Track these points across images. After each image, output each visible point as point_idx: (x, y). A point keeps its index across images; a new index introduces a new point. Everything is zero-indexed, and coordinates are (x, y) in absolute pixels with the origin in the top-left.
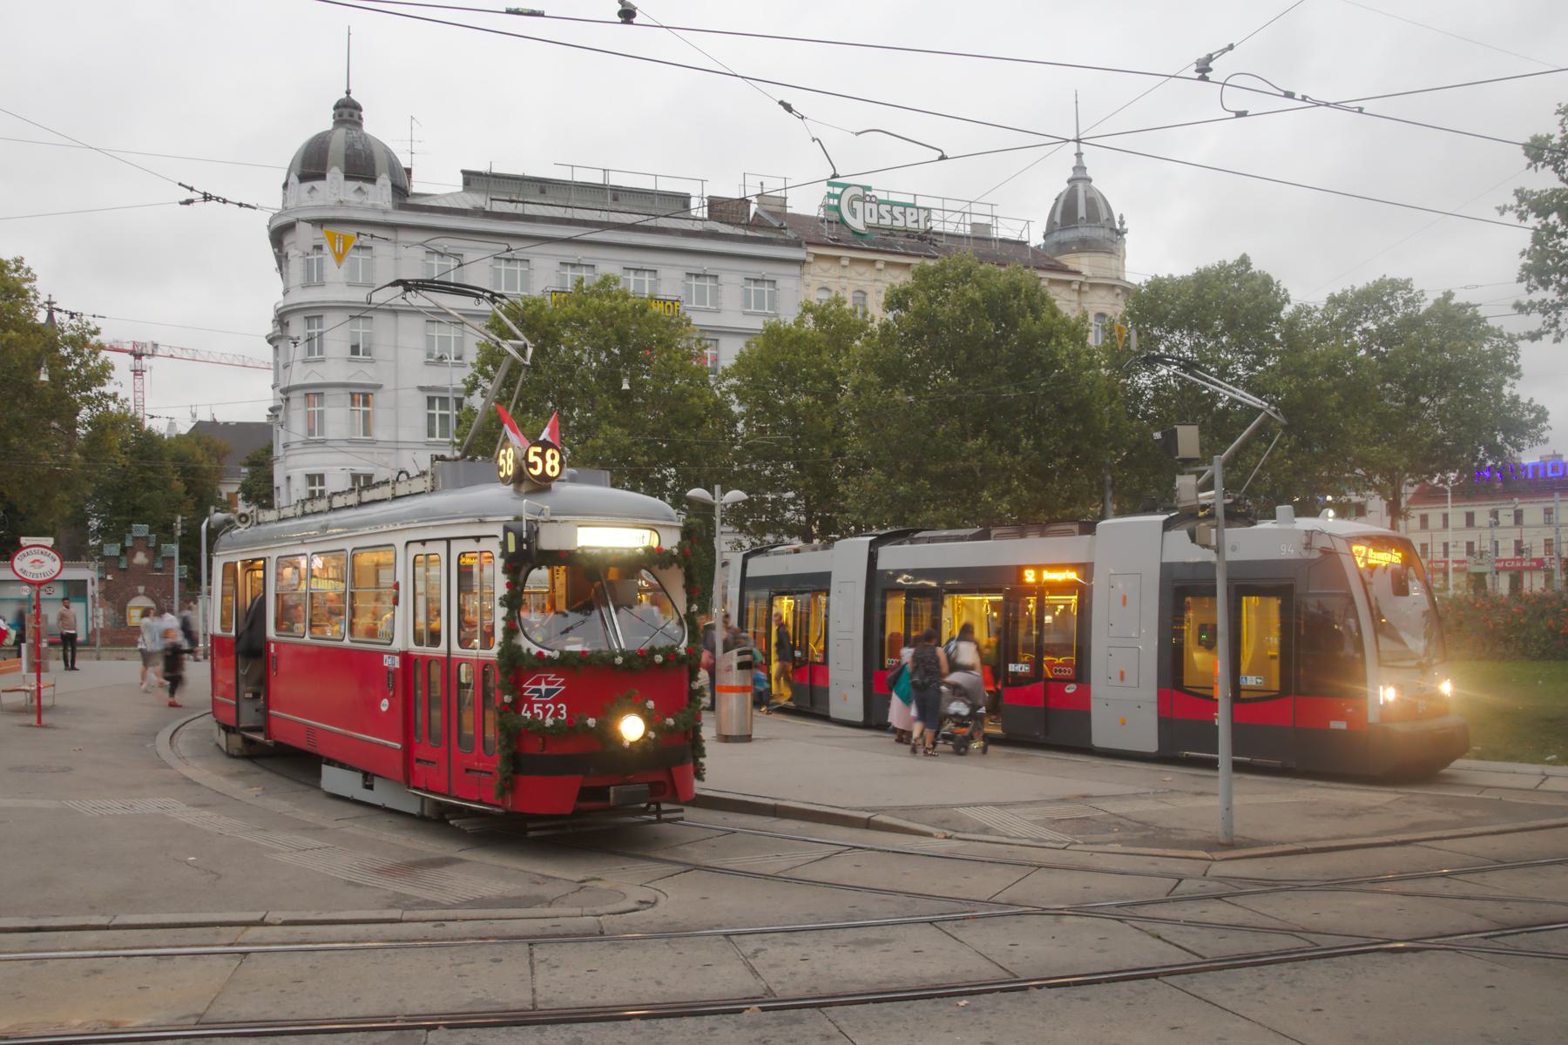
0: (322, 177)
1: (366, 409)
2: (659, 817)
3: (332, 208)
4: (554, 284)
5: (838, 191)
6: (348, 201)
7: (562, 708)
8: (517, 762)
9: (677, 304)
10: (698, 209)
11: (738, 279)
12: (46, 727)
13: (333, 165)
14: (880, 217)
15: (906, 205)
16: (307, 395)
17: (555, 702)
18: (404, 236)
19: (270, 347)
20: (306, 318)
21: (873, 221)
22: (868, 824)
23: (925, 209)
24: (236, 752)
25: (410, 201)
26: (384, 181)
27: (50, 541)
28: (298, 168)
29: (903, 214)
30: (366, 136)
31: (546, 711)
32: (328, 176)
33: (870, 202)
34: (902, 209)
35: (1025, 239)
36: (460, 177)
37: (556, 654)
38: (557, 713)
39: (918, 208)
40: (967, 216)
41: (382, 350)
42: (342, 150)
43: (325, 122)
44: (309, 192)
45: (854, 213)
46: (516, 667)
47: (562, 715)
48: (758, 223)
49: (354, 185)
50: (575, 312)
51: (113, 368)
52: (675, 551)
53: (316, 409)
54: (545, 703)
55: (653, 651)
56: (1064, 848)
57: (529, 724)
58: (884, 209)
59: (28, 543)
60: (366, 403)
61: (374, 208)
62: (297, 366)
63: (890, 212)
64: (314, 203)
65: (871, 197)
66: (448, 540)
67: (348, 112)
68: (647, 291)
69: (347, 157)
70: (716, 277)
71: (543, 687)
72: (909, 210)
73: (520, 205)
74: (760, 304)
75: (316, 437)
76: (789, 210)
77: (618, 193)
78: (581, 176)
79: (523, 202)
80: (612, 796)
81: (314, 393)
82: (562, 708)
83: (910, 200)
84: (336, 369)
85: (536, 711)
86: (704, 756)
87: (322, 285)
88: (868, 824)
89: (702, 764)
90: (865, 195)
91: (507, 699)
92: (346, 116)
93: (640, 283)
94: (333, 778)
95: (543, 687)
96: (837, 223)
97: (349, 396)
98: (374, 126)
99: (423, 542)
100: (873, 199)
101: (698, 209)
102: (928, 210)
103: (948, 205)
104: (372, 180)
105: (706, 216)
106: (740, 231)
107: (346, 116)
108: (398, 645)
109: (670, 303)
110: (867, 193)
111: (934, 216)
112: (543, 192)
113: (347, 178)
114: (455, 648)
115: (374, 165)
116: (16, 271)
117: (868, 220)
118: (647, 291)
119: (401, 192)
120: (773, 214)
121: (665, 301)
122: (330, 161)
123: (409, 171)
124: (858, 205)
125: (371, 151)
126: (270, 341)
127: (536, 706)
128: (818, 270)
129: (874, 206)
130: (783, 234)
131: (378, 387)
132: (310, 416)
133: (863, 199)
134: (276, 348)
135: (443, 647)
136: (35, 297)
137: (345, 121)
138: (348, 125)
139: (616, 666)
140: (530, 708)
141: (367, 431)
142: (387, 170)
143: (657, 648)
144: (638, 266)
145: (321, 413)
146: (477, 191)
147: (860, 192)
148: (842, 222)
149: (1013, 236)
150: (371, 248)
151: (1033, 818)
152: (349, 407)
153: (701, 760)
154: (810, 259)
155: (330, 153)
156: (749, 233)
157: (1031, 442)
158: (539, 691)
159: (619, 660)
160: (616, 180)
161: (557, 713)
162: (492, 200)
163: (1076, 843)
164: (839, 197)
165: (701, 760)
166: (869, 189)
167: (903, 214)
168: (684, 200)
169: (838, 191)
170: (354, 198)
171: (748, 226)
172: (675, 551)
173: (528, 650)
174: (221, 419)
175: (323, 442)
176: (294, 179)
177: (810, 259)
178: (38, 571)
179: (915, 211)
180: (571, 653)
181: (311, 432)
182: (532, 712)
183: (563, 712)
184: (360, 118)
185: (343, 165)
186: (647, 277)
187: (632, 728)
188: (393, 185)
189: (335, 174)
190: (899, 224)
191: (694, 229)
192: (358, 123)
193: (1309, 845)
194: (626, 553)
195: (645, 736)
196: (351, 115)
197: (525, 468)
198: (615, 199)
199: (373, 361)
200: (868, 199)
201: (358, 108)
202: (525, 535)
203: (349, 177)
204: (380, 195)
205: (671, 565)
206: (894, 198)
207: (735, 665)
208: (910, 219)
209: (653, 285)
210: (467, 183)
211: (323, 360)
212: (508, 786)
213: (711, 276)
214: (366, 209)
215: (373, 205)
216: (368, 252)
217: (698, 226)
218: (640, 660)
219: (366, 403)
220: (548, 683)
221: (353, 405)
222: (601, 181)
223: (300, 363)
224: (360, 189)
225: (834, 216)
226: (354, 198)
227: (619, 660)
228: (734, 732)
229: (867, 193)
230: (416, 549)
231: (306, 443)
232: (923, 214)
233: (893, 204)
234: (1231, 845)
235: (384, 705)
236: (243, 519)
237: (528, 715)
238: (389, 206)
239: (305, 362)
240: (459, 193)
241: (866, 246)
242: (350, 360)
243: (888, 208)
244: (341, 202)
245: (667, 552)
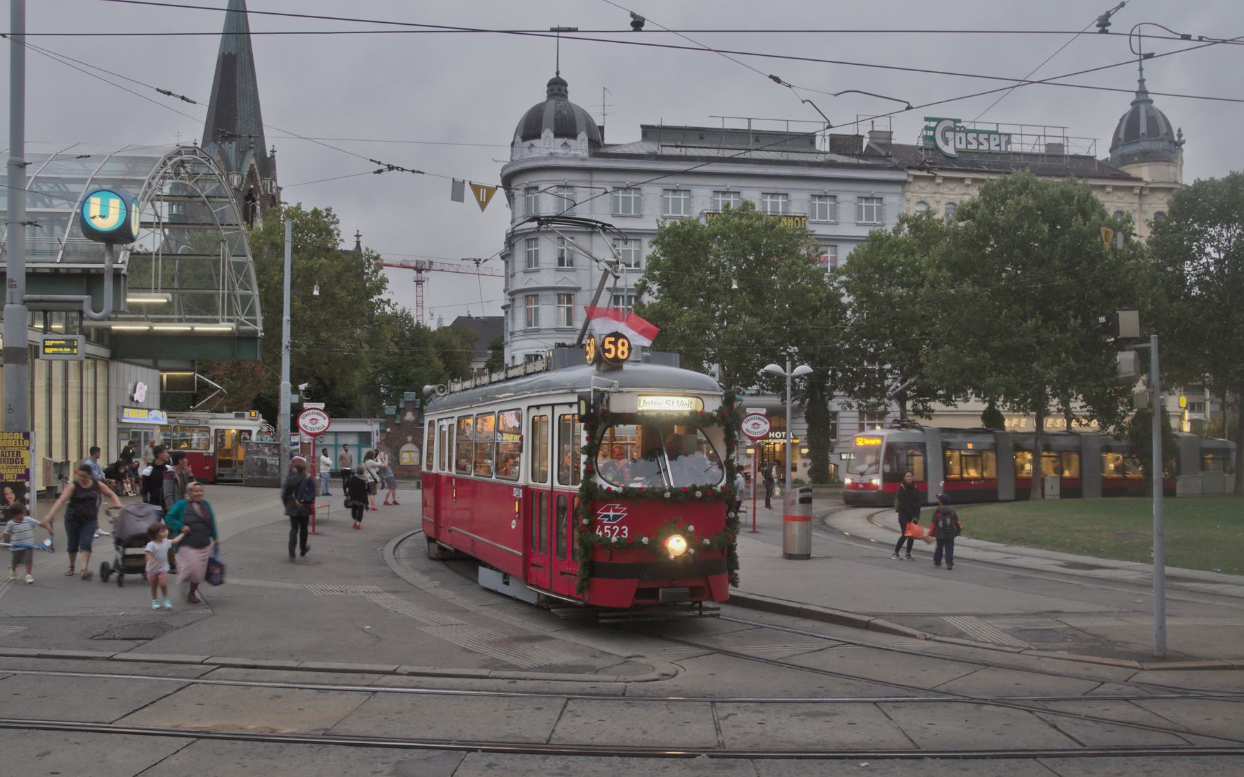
0: (538, 136)
1: (569, 305)
2: (700, 614)
3: (545, 159)
4: (709, 207)
5: (933, 124)
6: (557, 153)
7: (624, 529)
8: (592, 569)
9: (803, 219)
10: (822, 145)
11: (852, 198)
12: (317, 534)
14: (968, 143)
15: (989, 133)
16: (527, 296)
17: (620, 525)
18: (597, 177)
19: (503, 262)
21: (963, 146)
22: (868, 626)
23: (1006, 134)
24: (433, 556)
25: (602, 150)
26: (583, 136)
27: (322, 406)
28: (521, 131)
29: (988, 140)
30: (570, 104)
31: (613, 532)
32: (543, 135)
33: (960, 131)
34: (986, 136)
35: (1092, 154)
36: (640, 130)
37: (619, 490)
38: (621, 532)
39: (1000, 134)
40: (1042, 138)
41: (581, 260)
42: (553, 115)
43: (541, 97)
44: (529, 148)
45: (946, 142)
46: (593, 498)
47: (625, 535)
48: (870, 153)
49: (560, 141)
50: (720, 229)
51: (388, 282)
52: (715, 413)
53: (533, 306)
54: (612, 525)
55: (694, 488)
56: (1019, 652)
57: (600, 540)
58: (971, 136)
59: (309, 407)
60: (569, 301)
61: (575, 157)
62: (519, 276)
63: (977, 139)
65: (960, 128)
66: (553, 405)
67: (557, 87)
68: (780, 210)
69: (556, 120)
70: (835, 197)
71: (611, 514)
72: (992, 137)
73: (684, 149)
74: (869, 216)
75: (533, 327)
76: (893, 142)
77: (759, 136)
78: (730, 125)
79: (686, 147)
80: (660, 596)
81: (532, 295)
82: (624, 529)
83: (993, 128)
84: (547, 277)
85: (606, 531)
86: (738, 569)
88: (868, 626)
89: (736, 575)
90: (955, 126)
91: (585, 521)
92: (556, 91)
93: (775, 205)
94: (487, 577)
95: (611, 514)
96: (932, 150)
97: (556, 297)
98: (576, 97)
99: (538, 407)
100: (962, 129)
101: (822, 145)
102: (1009, 135)
103: (1026, 130)
104: (574, 136)
105: (828, 149)
106: (854, 160)
107: (556, 91)
108: (521, 482)
109: (797, 219)
110: (957, 124)
111: (1013, 140)
112: (701, 138)
113: (557, 135)
114: (556, 484)
115: (575, 125)
116: (326, 217)
117: (958, 146)
118: (780, 210)
119: (596, 144)
120: (881, 145)
121: (794, 217)
123: (602, 128)
124: (949, 135)
125: (574, 116)
126: (503, 258)
127: (606, 527)
128: (917, 188)
129: (963, 135)
130: (889, 161)
131: (578, 289)
132: (528, 311)
133: (953, 130)
134: (507, 262)
135: (548, 483)
136: (338, 235)
137: (557, 95)
138: (558, 97)
139: (665, 499)
140: (602, 529)
141: (569, 322)
143: (698, 486)
144: (773, 191)
145: (537, 310)
146: (652, 140)
147: (951, 124)
148: (936, 149)
149: (1083, 153)
151: (1005, 627)
152: (556, 304)
153: (736, 571)
154: (911, 179)
155: (544, 119)
156: (861, 161)
157: (1079, 321)
158: (608, 516)
159: (668, 495)
160: (756, 126)
161: (621, 532)
162: (662, 146)
163: (1031, 649)
164: (934, 129)
165: (736, 571)
166: (959, 121)
167: (988, 140)
168: (810, 138)
169: (933, 124)
170: (561, 151)
171: (861, 156)
172: (715, 413)
173: (601, 486)
174: (475, 314)
175: (539, 330)
176: (519, 139)
177: (911, 179)
178: (314, 426)
179: (997, 137)
180: (632, 488)
181: (529, 324)
182: (603, 531)
183: (625, 532)
184: (566, 92)
185: (553, 128)
186: (780, 200)
187: (677, 545)
188: (589, 140)
189: (548, 133)
190: (984, 147)
191: (818, 160)
192: (564, 95)
193: (1235, 663)
194: (676, 414)
195: (687, 552)
196: (560, 90)
197: (602, 353)
198: (757, 140)
199: (574, 270)
200: (958, 129)
201: (564, 84)
202: (592, 403)
203: (557, 135)
204: (580, 147)
205: (712, 424)
206: (979, 127)
207: (797, 499)
208: (993, 143)
209: (786, 205)
210: (645, 135)
211: (538, 271)
212: (585, 586)
213: (831, 196)
215: (575, 155)
216: (571, 189)
217: (821, 158)
218: (684, 495)
219: (569, 301)
220: (614, 511)
221: (559, 303)
222: (746, 127)
224: (565, 144)
225: (931, 145)
226: (561, 151)
227: (668, 495)
228: (796, 551)
229: (957, 124)
230: (534, 412)
231: (525, 332)
232: (1004, 139)
233: (978, 132)
234: (1164, 658)
235: (514, 525)
236: (442, 390)
237: (601, 534)
238: (586, 155)
239: (525, 272)
240: (638, 142)
241: (956, 167)
242: (557, 270)
243: (975, 135)
245: (708, 414)
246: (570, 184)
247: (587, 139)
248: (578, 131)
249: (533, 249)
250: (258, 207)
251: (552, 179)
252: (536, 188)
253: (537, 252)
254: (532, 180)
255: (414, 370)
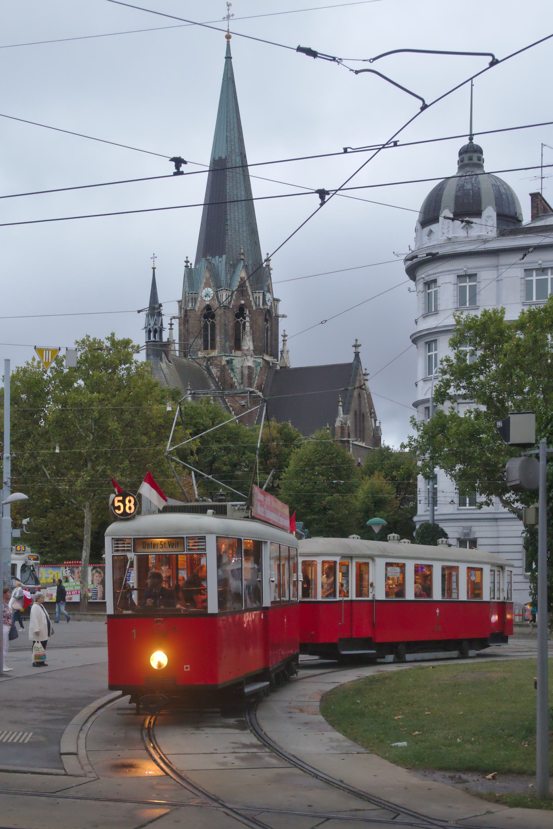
0: (435, 220)
3: (441, 246)
13: (444, 208)
18: (505, 260)
20: (426, 343)
42: (453, 193)
43: (452, 169)
64: (432, 244)
69: (457, 198)
87: (436, 312)
92: (466, 161)
107: (466, 161)
122: (443, 204)
125: (479, 188)
142: (494, 202)
150: (476, 275)
155: (443, 198)
176: (419, 227)
188: (498, 215)
214: (470, 242)
223: (422, 382)
244: (450, 239)
246: (470, 272)
247: (495, 214)
248: (483, 206)
249: (433, 353)
250: (248, 324)
251: (451, 268)
252: (435, 281)
253: (436, 355)
254: (431, 272)
255: (329, 498)
